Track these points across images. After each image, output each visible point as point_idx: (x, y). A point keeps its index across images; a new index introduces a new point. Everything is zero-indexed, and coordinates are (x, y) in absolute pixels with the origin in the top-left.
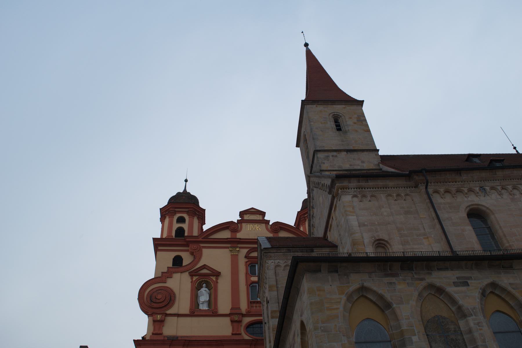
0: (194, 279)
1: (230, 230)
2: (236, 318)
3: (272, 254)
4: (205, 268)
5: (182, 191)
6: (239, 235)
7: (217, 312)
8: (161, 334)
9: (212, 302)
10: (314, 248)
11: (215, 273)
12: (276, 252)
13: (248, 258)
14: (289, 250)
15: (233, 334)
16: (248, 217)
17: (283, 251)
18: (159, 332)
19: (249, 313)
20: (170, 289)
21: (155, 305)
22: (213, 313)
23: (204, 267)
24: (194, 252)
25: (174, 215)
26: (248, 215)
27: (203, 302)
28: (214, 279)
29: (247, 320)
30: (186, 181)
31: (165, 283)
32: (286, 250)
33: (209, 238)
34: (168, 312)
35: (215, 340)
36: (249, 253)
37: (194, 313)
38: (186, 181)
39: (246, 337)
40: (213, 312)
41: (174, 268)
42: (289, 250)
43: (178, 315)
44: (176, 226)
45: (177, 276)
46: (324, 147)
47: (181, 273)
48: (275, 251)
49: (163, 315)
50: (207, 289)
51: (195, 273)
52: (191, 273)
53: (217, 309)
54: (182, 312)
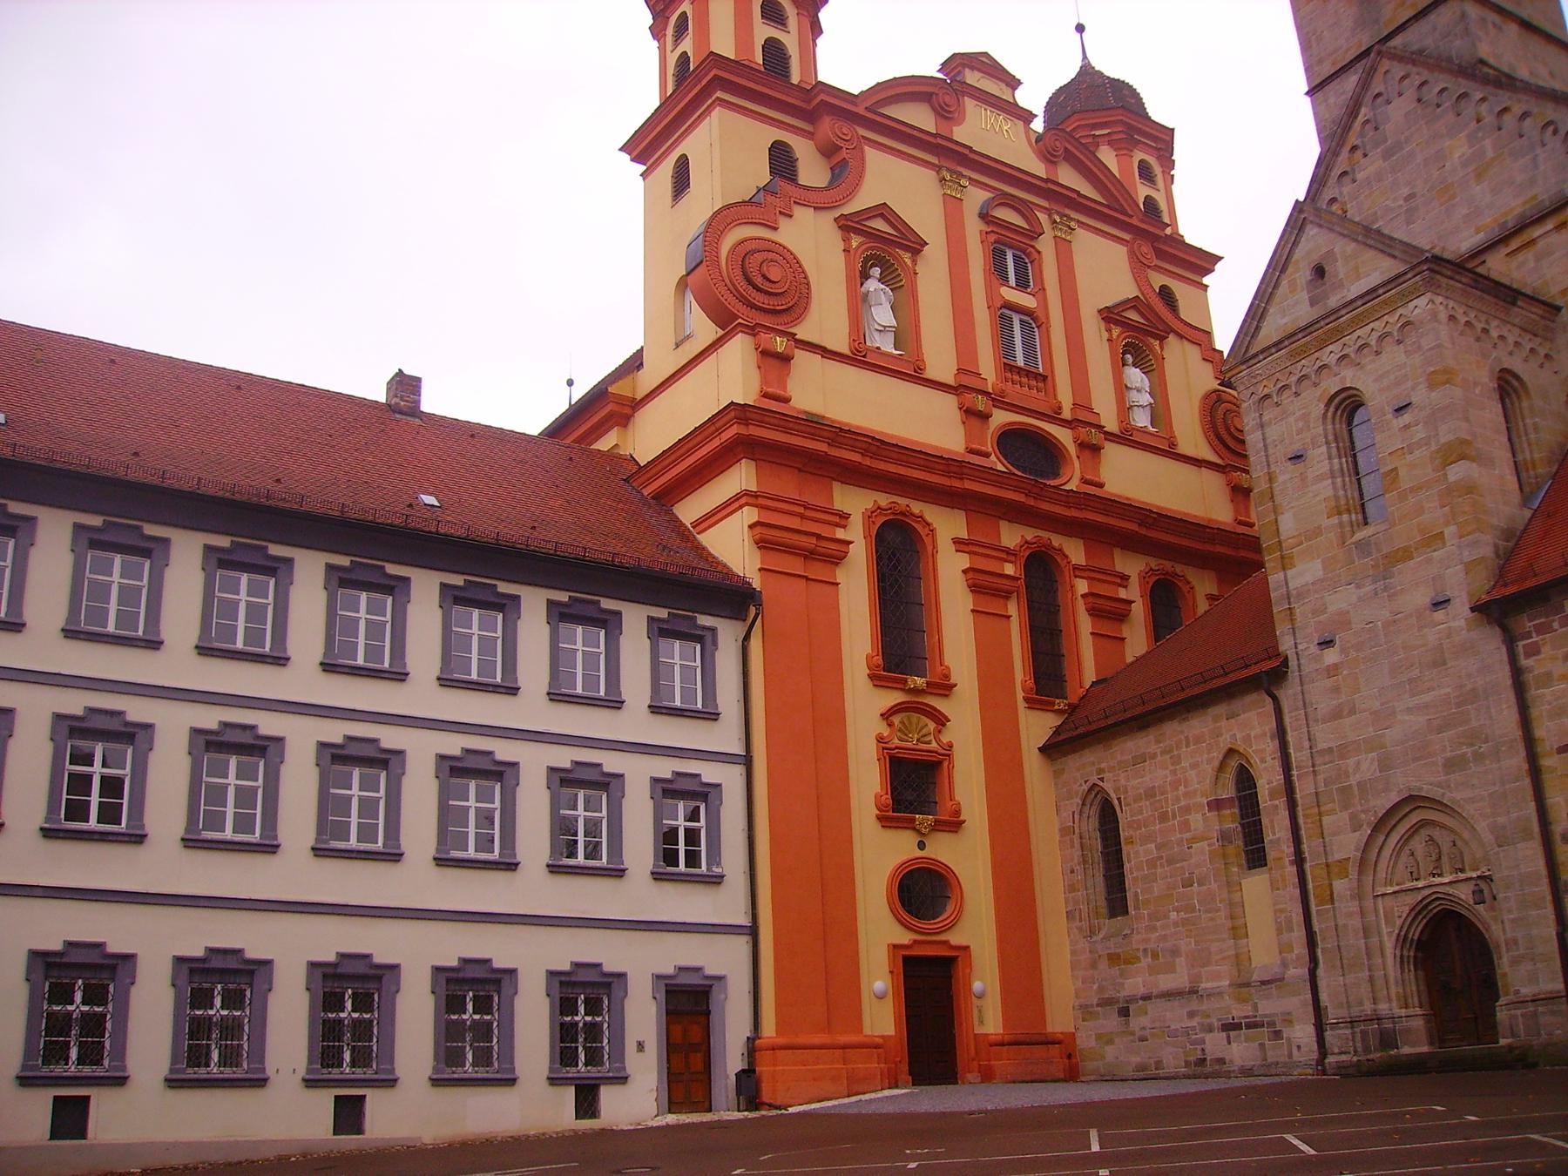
0: (854, 245)
1: (934, 109)
2: (981, 403)
3: (1444, 281)
4: (882, 215)
6: (961, 134)
8: (787, 400)
9: (908, 333)
12: (1452, 278)
13: (988, 223)
14: (1476, 281)
17: (1464, 280)
20: (792, 257)
21: (760, 299)
23: (883, 211)
26: (977, 75)
27: (885, 327)
28: (908, 261)
31: (775, 229)
33: (882, 111)
51: (857, 222)
52: (847, 220)
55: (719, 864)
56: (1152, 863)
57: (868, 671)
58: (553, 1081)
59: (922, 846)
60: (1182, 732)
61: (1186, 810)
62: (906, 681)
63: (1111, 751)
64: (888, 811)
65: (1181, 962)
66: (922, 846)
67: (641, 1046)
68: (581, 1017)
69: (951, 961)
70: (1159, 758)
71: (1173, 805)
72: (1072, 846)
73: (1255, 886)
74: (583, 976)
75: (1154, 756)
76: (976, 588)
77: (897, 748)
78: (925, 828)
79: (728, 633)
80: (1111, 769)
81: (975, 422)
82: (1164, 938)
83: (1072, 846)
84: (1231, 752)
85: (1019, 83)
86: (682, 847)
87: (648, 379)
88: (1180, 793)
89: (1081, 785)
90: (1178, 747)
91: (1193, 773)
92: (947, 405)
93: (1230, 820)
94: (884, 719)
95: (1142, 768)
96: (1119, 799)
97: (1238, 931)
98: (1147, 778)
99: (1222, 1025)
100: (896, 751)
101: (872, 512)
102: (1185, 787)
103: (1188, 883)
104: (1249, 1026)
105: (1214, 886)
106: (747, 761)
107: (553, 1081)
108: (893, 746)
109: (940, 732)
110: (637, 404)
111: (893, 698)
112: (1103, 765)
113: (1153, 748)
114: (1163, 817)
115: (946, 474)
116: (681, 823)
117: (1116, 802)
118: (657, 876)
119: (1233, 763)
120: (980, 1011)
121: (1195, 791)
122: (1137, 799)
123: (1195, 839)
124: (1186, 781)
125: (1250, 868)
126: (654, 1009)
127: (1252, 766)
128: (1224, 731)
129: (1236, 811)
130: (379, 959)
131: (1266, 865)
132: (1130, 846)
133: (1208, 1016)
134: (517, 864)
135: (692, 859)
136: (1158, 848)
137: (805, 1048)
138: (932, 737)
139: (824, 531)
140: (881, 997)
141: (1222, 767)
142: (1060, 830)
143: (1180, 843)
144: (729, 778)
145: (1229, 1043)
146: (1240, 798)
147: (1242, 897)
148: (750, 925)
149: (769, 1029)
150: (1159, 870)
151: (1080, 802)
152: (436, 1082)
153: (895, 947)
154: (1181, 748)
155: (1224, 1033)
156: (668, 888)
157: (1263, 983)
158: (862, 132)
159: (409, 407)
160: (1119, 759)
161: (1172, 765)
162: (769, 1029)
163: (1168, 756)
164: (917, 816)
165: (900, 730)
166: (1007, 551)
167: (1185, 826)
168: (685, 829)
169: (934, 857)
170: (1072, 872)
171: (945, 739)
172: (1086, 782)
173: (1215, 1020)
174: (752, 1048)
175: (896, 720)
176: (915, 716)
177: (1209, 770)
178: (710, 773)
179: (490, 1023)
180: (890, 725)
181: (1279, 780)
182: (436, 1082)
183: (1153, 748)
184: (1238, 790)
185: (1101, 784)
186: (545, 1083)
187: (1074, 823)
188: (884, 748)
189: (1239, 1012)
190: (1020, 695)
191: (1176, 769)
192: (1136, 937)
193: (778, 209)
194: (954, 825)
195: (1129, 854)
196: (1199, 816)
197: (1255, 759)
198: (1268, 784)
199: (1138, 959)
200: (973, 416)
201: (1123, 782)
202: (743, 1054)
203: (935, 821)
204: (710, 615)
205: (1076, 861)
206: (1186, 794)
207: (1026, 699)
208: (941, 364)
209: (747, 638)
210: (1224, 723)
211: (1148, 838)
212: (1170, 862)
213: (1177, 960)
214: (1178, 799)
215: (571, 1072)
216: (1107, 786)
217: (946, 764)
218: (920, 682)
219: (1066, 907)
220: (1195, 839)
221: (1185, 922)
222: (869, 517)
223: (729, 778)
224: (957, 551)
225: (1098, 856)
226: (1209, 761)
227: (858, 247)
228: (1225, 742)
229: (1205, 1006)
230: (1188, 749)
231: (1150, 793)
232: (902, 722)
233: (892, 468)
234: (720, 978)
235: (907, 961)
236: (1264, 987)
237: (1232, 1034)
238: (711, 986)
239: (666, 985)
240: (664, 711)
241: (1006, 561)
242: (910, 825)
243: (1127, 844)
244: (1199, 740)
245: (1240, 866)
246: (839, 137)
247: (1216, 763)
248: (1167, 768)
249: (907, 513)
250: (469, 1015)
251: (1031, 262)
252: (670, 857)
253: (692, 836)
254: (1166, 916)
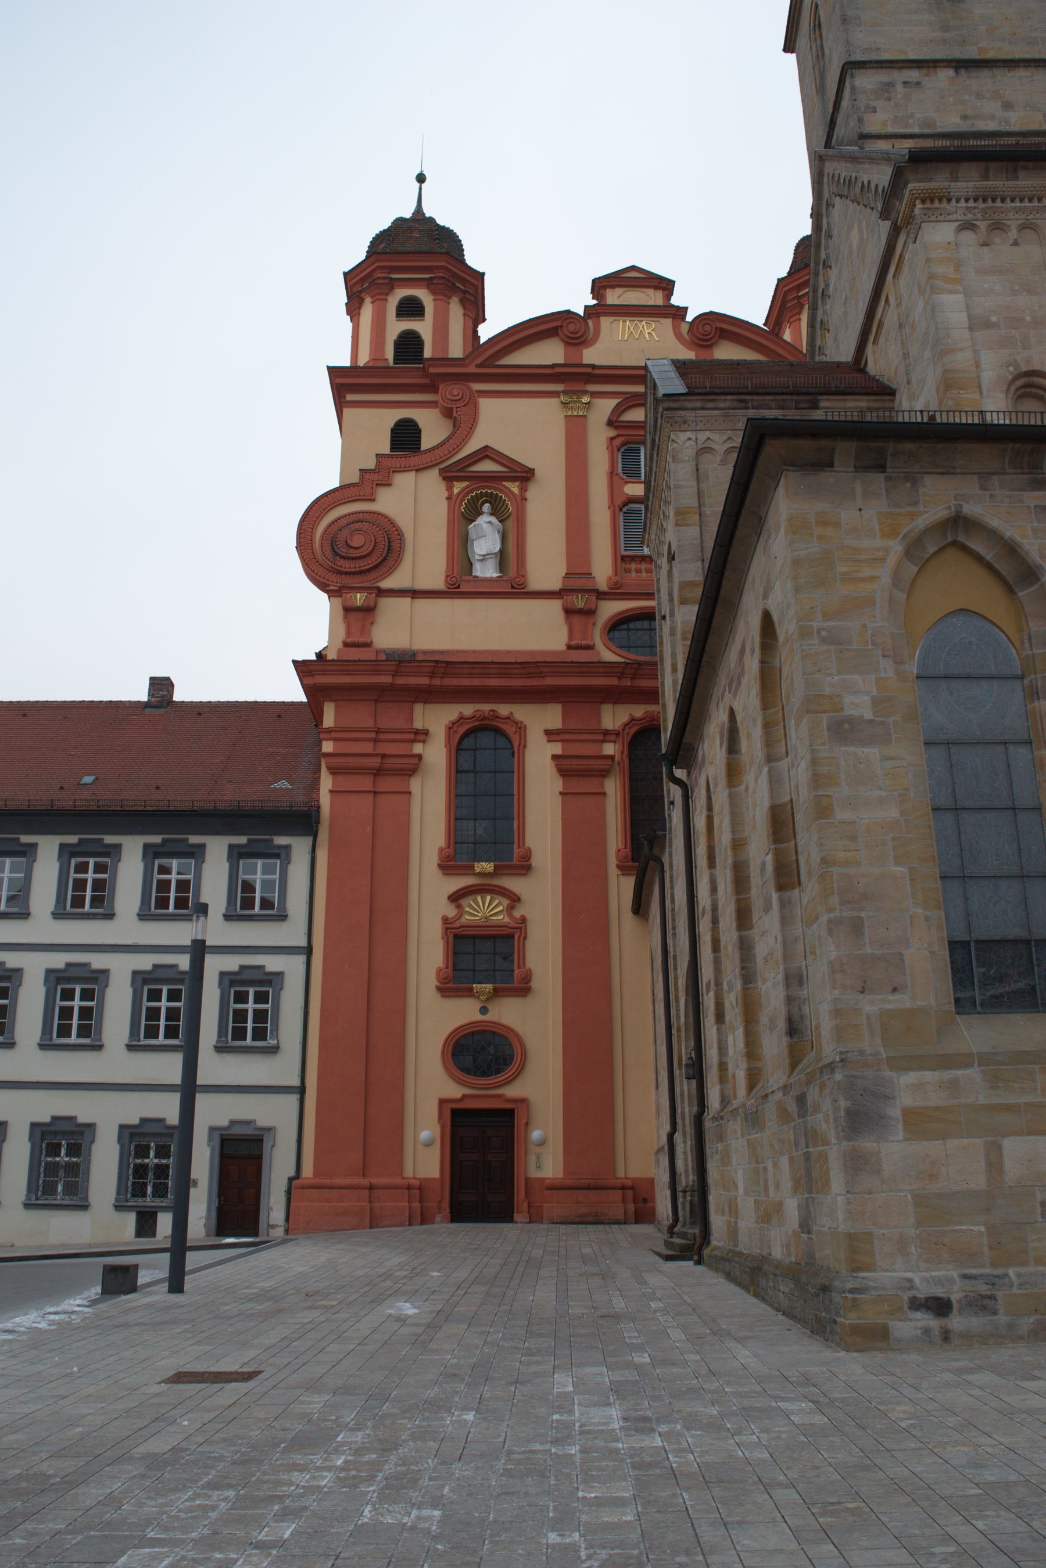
0: (456, 491)
1: (563, 341)
2: (579, 602)
3: (690, 415)
4: (487, 457)
5: (408, 215)
6: (592, 356)
7: (523, 585)
8: (368, 645)
10: (820, 397)
11: (516, 471)
13: (616, 428)
14: (741, 401)
15: (570, 647)
16: (619, 297)
17: (722, 405)
18: (361, 640)
19: (619, 588)
21: (347, 566)
22: (513, 587)
23: (485, 453)
24: (454, 409)
25: (387, 294)
26: (618, 291)
27: (484, 555)
29: (611, 609)
30: (421, 179)
31: (373, 500)
32: (732, 400)
34: (386, 584)
35: (519, 661)
36: (618, 410)
37: (458, 587)
38: (421, 179)
39: (608, 656)
40: (515, 586)
41: (397, 457)
42: (741, 401)
43: (415, 594)
44: (396, 327)
45: (404, 481)
46: (878, 49)
47: (417, 470)
48: (698, 404)
49: (371, 594)
50: (493, 519)
51: (458, 471)
52: (446, 472)
53: (523, 576)
54: (422, 585)
58: (118, 1207)
62: (473, 867)
66: (484, 1010)
68: (152, 1160)
69: (509, 1113)
76: (564, 772)
79: (300, 846)
85: (672, 283)
106: (308, 951)
107: (118, 1207)
115: (501, 675)
120: (538, 1157)
126: (208, 1154)
130: (81, 1120)
137: (331, 1188)
140: (429, 1144)
144: (292, 967)
149: (308, 1171)
152: (27, 1206)
153: (442, 1102)
158: (477, 387)
159: (158, 702)
162: (308, 1171)
166: (606, 732)
178: (272, 963)
179: (167, 1166)
182: (27, 1206)
186: (112, 1209)
190: (612, 861)
193: (375, 483)
194: (523, 989)
207: (618, 866)
215: (140, 1202)
222: (451, 728)
223: (292, 967)
224: (549, 741)
227: (459, 494)
233: (466, 682)
234: (269, 1129)
235: (455, 1112)
239: (221, 1135)
241: (604, 741)
242: (469, 993)
246: (452, 400)
249: (495, 716)
250: (63, 1158)
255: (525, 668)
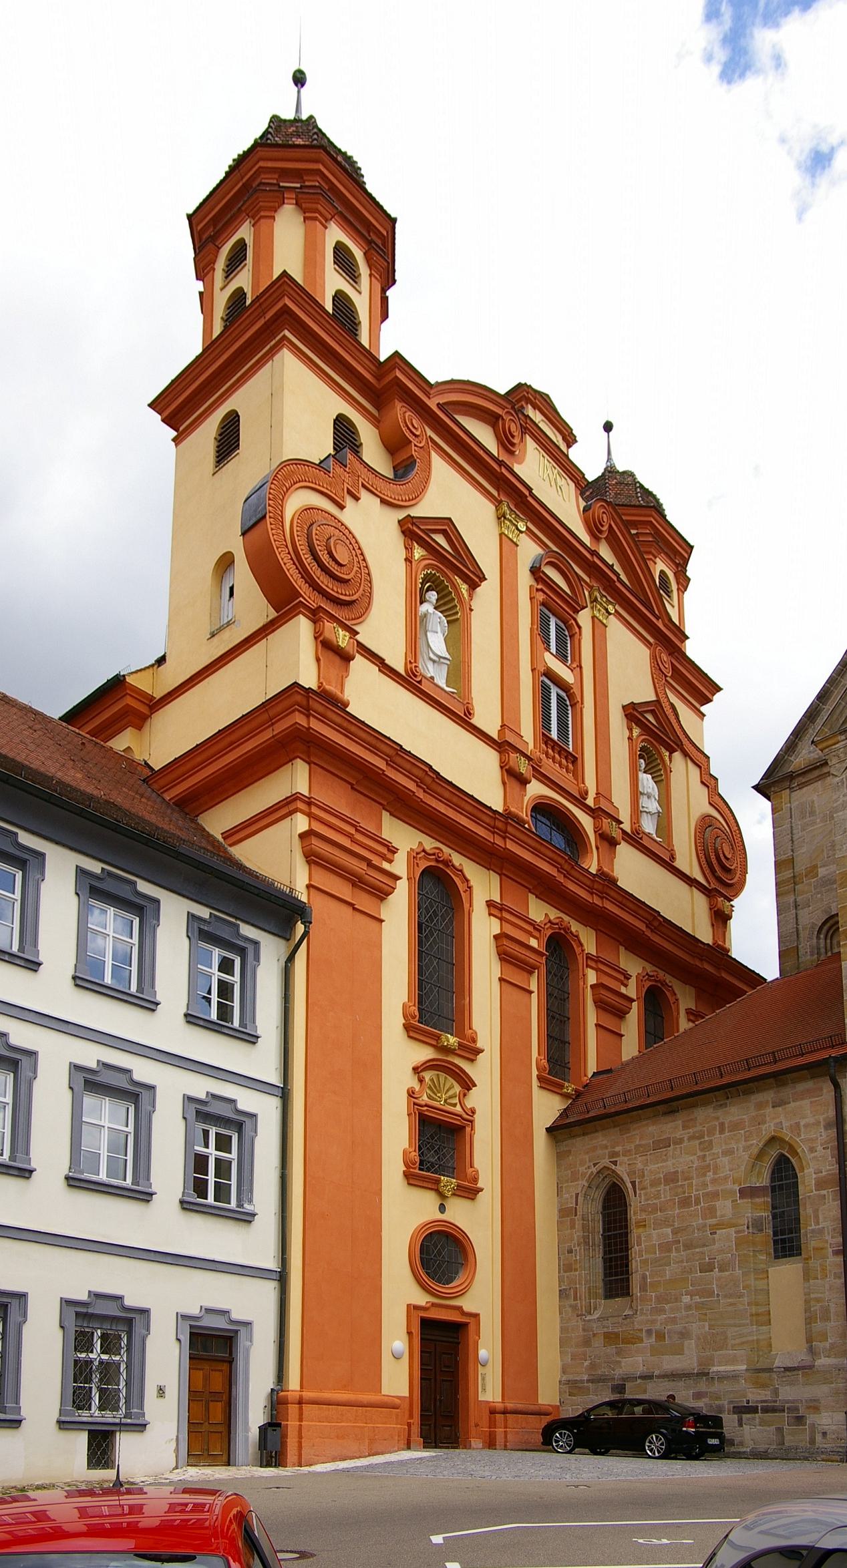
55: (250, 1201)
56: (666, 1247)
57: (404, 1021)
59: (442, 1208)
60: (718, 1118)
61: (715, 1195)
63: (628, 1135)
64: (415, 1168)
65: (690, 1345)
67: (161, 1391)
70: (686, 1143)
71: (697, 1190)
72: (573, 1227)
73: (786, 1273)
74: (101, 1308)
75: (681, 1141)
77: (426, 1105)
78: (449, 1191)
80: (627, 1153)
81: (513, 785)
82: (673, 1321)
83: (573, 1227)
84: (773, 1140)
86: (211, 1178)
87: (172, 676)
88: (708, 1179)
89: (589, 1167)
90: (711, 1132)
91: (725, 1160)
92: (490, 759)
93: (759, 1209)
94: (415, 1073)
95: (664, 1153)
96: (633, 1183)
97: (764, 1318)
98: (669, 1163)
99: (734, 1407)
100: (425, 1108)
101: (417, 854)
102: (715, 1173)
103: (707, 1268)
104: (766, 1410)
105: (738, 1272)
106: (285, 1094)
108: (423, 1103)
109: (465, 1095)
110: (156, 704)
111: (424, 1053)
112: (617, 1149)
113: (679, 1134)
114: (685, 1202)
116: (212, 1152)
117: (629, 1185)
118: (185, 1205)
119: (774, 1153)
121: (726, 1178)
122: (654, 1183)
123: (720, 1225)
124: (716, 1167)
125: (776, 1257)
127: (795, 1153)
128: (768, 1119)
129: (770, 1200)
131: (800, 1254)
132: (641, 1230)
133: (718, 1398)
134: (31, 1172)
135: (222, 1192)
136: (675, 1232)
138: (456, 1101)
139: (376, 860)
141: (760, 1155)
142: (560, 1211)
143: (701, 1228)
145: (741, 1425)
146: (773, 1189)
147: (768, 1285)
148: (279, 1270)
150: (674, 1254)
151: (586, 1184)
154: (714, 1135)
155: (736, 1416)
156: (198, 1221)
157: (787, 1369)
160: (637, 1143)
161: (701, 1150)
163: (697, 1142)
164: (442, 1178)
165: (430, 1088)
167: (712, 1211)
168: (216, 1159)
169: (452, 1221)
170: (570, 1251)
171: (469, 1103)
172: (595, 1165)
173: (726, 1402)
174: (277, 1402)
175: (428, 1076)
176: (442, 1075)
177: (745, 1157)
178: (247, 1100)
180: (421, 1081)
181: (833, 1169)
183: (679, 1134)
184: (773, 1179)
185: (614, 1167)
187: (577, 1205)
188: (415, 1104)
189: (755, 1395)
191: (705, 1155)
192: (639, 1318)
194: (470, 1192)
195: (639, 1237)
196: (728, 1203)
197: (803, 1149)
198: (815, 1173)
199: (641, 1341)
200: (513, 777)
201: (640, 1166)
202: (265, 1407)
203: (458, 1186)
204: (253, 925)
205: (576, 1241)
206: (714, 1181)
208: (488, 718)
209: (291, 959)
210: (769, 1110)
211: (666, 1222)
212: (688, 1246)
213: (686, 1343)
214: (705, 1185)
216: (621, 1170)
217: (468, 1129)
218: (452, 1040)
219: (560, 1286)
220: (720, 1225)
221: (698, 1306)
223: (266, 1109)
225: (599, 1238)
226: (746, 1149)
228: (768, 1129)
229: (716, 1387)
230: (722, 1136)
231: (671, 1178)
232: (432, 1080)
234: (248, 1324)
236: (788, 1373)
237: (745, 1416)
238: (236, 1332)
240: (201, 1023)
243: (638, 1227)
244: (735, 1127)
245: (768, 1254)
247: (755, 1151)
248: (695, 1154)
251: (570, 637)
252: (200, 1188)
253: (223, 1168)
254: (677, 1300)
255: (495, 818)
